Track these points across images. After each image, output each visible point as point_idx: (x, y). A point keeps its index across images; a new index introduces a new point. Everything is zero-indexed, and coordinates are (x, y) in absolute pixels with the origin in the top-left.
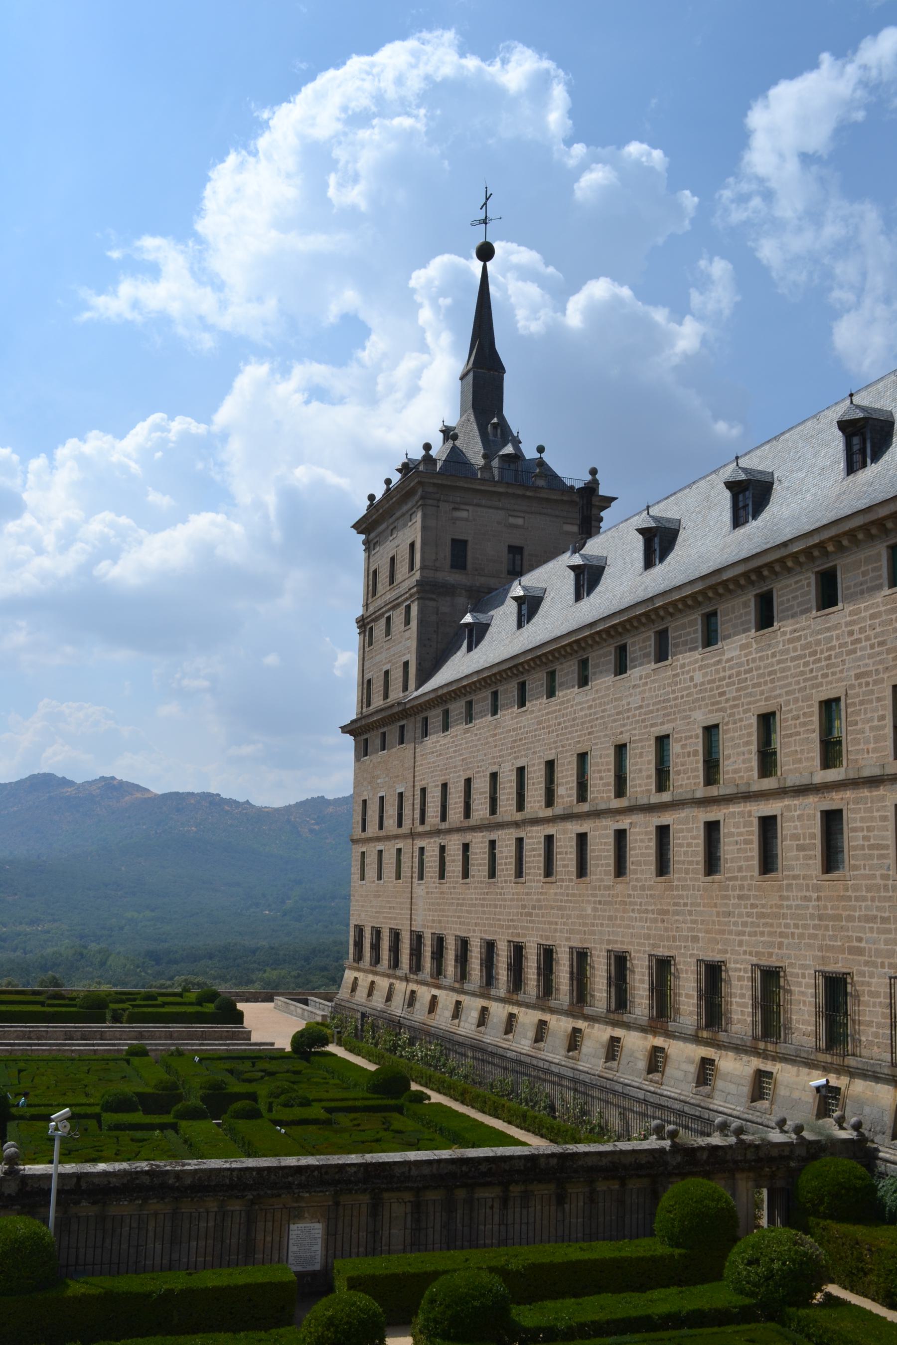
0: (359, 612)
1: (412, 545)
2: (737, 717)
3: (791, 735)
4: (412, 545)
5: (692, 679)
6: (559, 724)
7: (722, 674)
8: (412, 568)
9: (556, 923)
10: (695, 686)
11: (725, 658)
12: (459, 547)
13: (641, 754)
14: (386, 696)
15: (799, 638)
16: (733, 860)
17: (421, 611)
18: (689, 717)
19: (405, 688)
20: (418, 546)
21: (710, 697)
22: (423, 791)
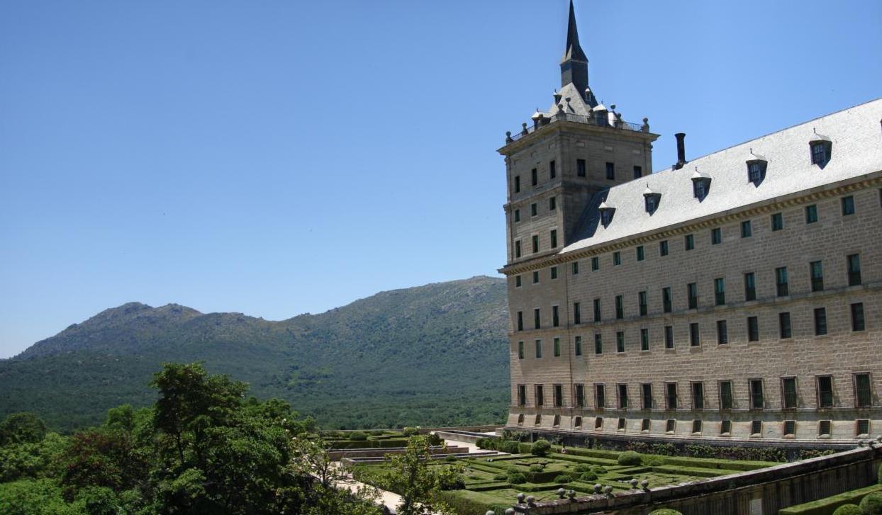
0: (506, 202)
1: (553, 164)
2: (832, 257)
3: (869, 265)
4: (553, 164)
5: (800, 239)
6: (698, 263)
7: (821, 236)
8: (553, 175)
9: (703, 369)
10: (803, 242)
11: (823, 228)
12: (581, 163)
13: (765, 278)
14: (536, 250)
15: (871, 219)
16: (834, 326)
17: (565, 201)
18: (800, 258)
19: (554, 244)
20: (558, 162)
21: (814, 248)
22: (577, 305)
